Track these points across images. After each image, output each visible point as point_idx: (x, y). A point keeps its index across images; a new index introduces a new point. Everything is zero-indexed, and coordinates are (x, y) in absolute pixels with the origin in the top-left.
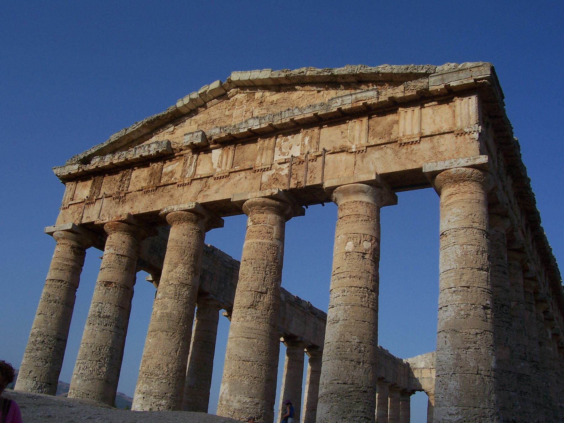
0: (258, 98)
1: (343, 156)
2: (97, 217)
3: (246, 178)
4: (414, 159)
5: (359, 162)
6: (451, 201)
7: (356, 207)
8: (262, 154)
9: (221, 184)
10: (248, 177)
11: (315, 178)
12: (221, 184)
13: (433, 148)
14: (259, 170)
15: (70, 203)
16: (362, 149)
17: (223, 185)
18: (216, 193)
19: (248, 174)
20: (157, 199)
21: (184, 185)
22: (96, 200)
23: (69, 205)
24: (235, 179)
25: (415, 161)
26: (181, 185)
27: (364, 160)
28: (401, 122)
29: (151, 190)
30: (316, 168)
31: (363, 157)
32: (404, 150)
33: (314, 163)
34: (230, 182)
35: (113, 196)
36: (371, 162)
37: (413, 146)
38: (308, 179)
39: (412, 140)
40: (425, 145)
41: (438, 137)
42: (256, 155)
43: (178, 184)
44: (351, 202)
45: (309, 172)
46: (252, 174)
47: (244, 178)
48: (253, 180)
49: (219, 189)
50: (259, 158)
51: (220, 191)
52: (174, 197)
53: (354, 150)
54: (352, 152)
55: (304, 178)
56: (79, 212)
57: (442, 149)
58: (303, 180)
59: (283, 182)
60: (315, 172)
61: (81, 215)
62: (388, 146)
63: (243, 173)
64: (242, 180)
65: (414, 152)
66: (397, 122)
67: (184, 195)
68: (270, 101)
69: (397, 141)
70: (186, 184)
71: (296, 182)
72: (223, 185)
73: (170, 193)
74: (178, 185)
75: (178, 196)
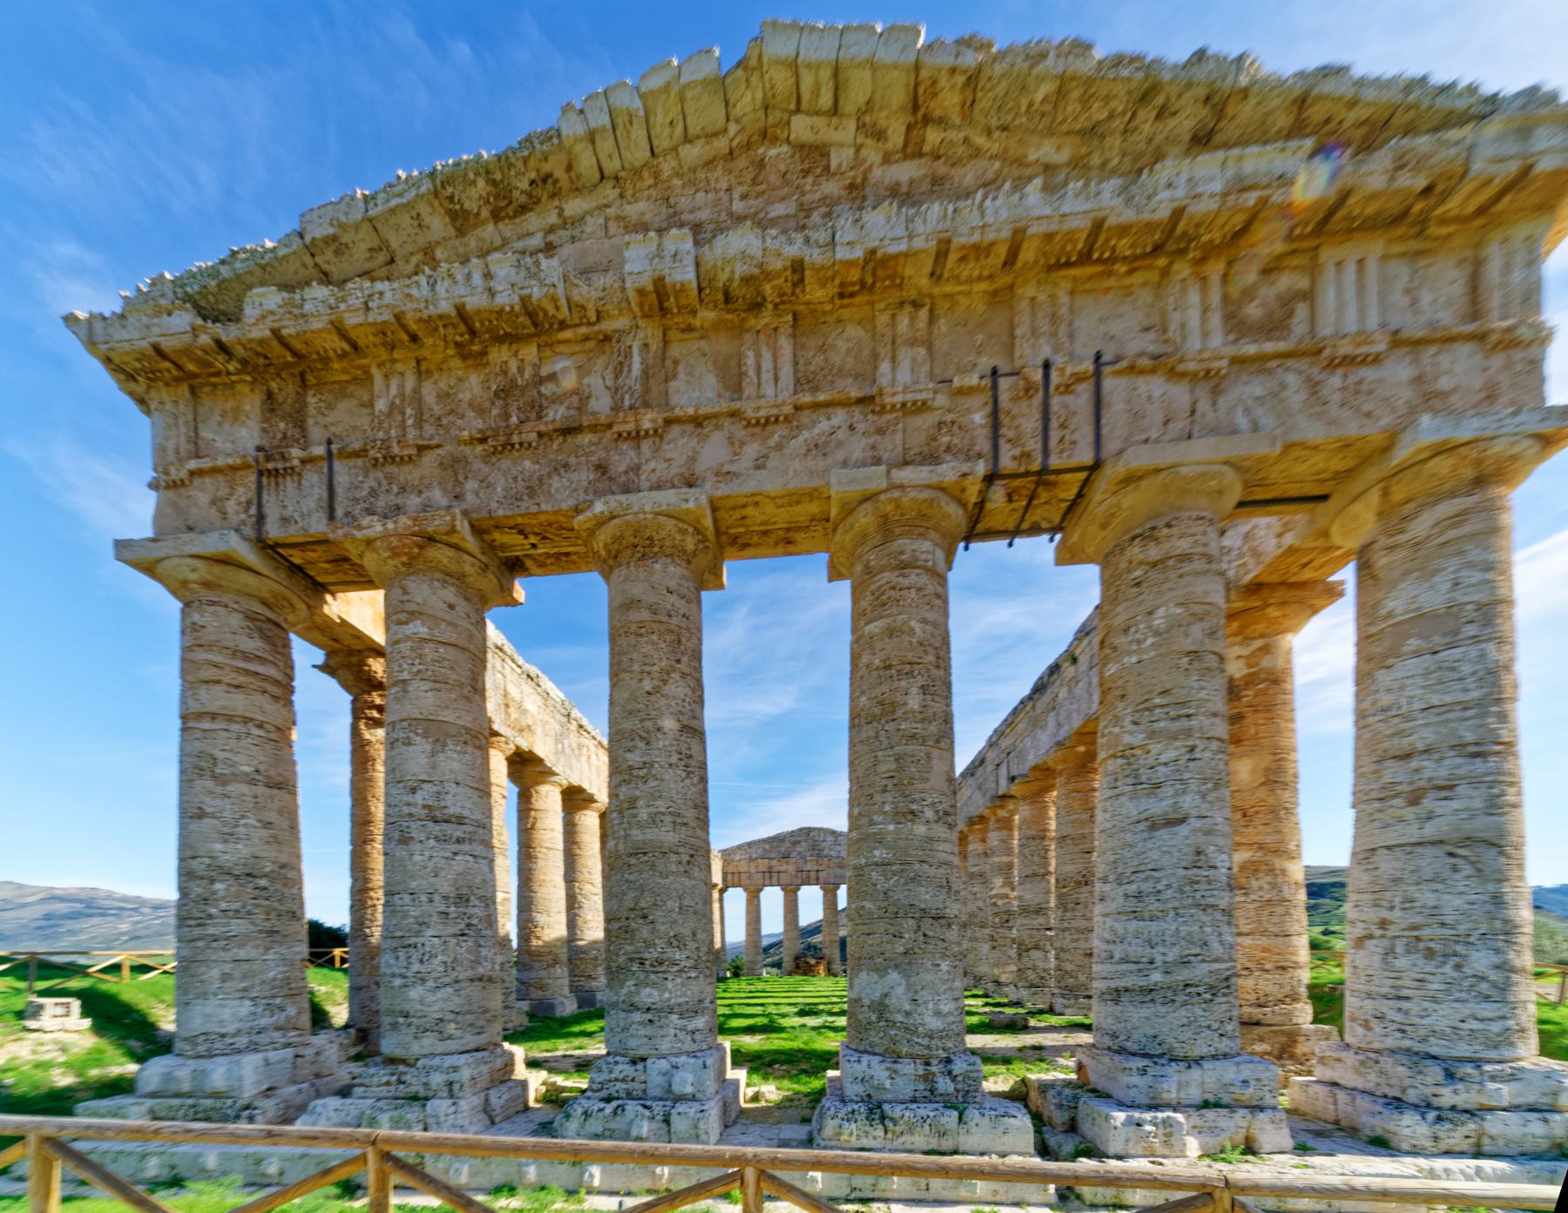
0: (840, 165)
1: (1156, 386)
2: (324, 521)
3: (851, 428)
4: (1366, 408)
5: (1203, 406)
6: (1466, 529)
7: (1204, 533)
8: (894, 360)
9: (772, 442)
10: (861, 427)
11: (1074, 443)
12: (772, 442)
13: (1418, 380)
14: (893, 406)
15: (193, 464)
16: (1216, 364)
17: (779, 447)
18: (758, 468)
19: (858, 416)
20: (549, 475)
21: (637, 437)
22: (303, 462)
23: (192, 473)
24: (816, 431)
25: (1368, 415)
26: (629, 433)
27: (1221, 400)
28: (1328, 296)
29: (521, 444)
30: (1074, 414)
31: (1216, 391)
32: (1336, 381)
33: (1069, 399)
34: (801, 438)
35: (372, 453)
36: (1240, 410)
37: (1368, 373)
38: (1053, 442)
39: (1364, 350)
40: (1398, 372)
41: (1433, 349)
42: (875, 356)
43: (615, 428)
44: (1189, 518)
45: (1054, 423)
46: (870, 417)
47: (845, 428)
48: (879, 438)
49: (766, 457)
50: (885, 367)
51: (771, 464)
52: (612, 473)
53: (1192, 366)
54: (1183, 375)
55: (1039, 439)
56: (243, 499)
57: (1444, 384)
58: (1039, 446)
59: (977, 448)
60: (1073, 426)
61: (253, 510)
62: (1289, 363)
63: (839, 417)
64: (841, 435)
65: (1364, 387)
66: (1308, 296)
67: (644, 467)
68: (887, 182)
69: (1320, 351)
70: (647, 432)
71: (1017, 452)
72: (779, 447)
73: (594, 458)
74: (620, 435)
75: (622, 468)
